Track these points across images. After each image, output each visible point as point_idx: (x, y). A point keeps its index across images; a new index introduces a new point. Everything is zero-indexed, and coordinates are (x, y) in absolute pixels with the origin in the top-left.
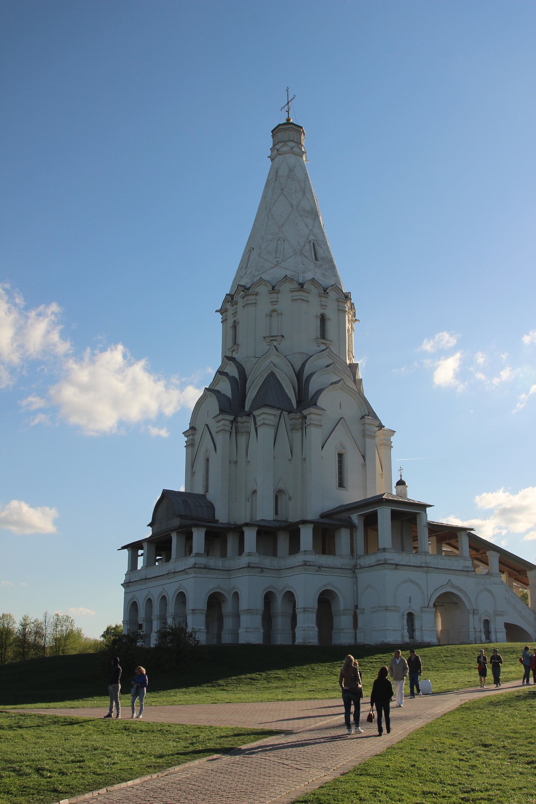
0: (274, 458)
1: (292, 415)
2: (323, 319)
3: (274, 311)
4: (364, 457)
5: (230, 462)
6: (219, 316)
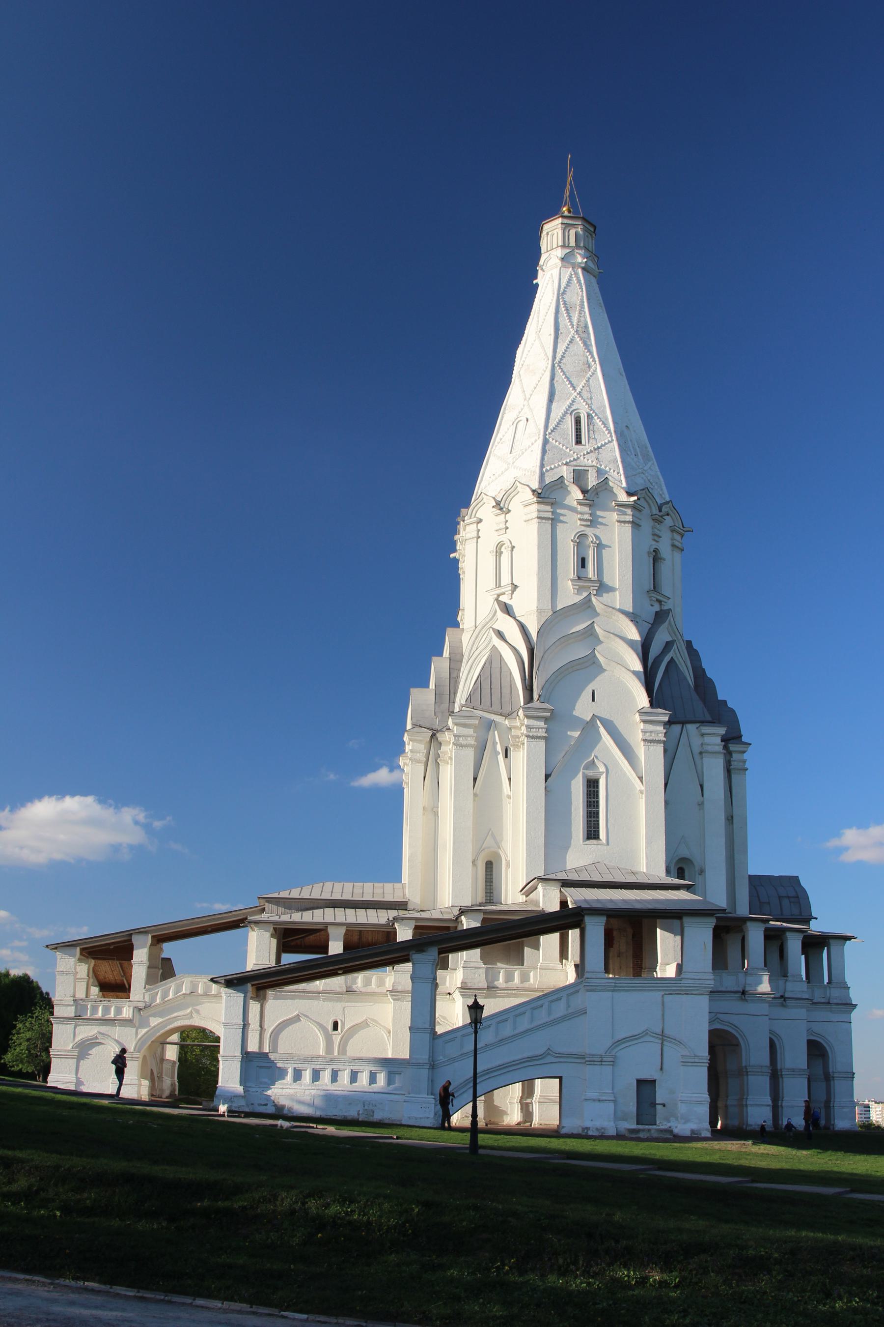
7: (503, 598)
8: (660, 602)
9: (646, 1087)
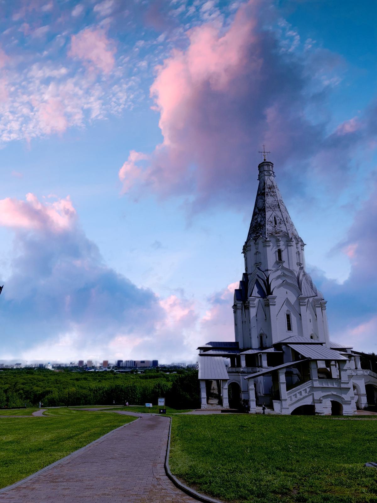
1: (265, 299)
2: (280, 252)
3: (257, 252)
4: (300, 315)
5: (242, 322)
6: (243, 254)
7: (258, 266)
8: (300, 265)
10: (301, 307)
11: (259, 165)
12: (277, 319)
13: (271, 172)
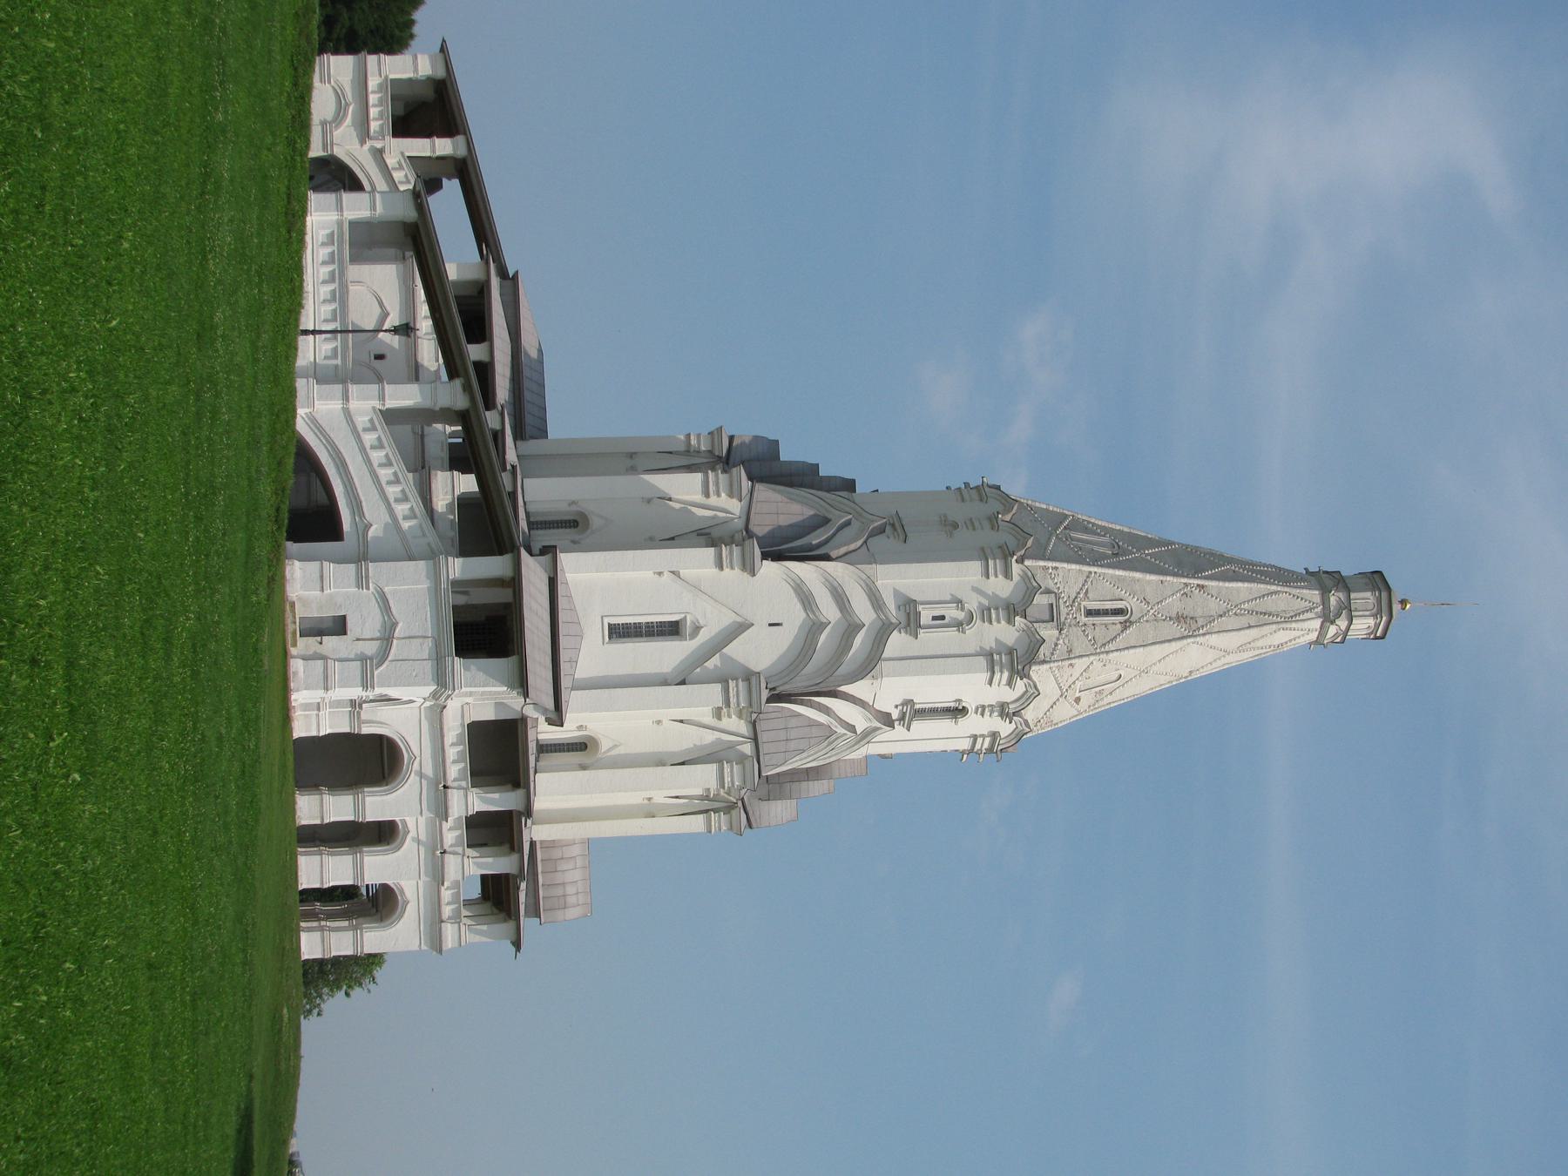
0: (649, 501)
3: (955, 526)
5: (631, 455)
7: (888, 529)
8: (902, 718)
9: (339, 626)
10: (718, 687)
11: (1380, 573)
12: (660, 574)
13: (1342, 623)
